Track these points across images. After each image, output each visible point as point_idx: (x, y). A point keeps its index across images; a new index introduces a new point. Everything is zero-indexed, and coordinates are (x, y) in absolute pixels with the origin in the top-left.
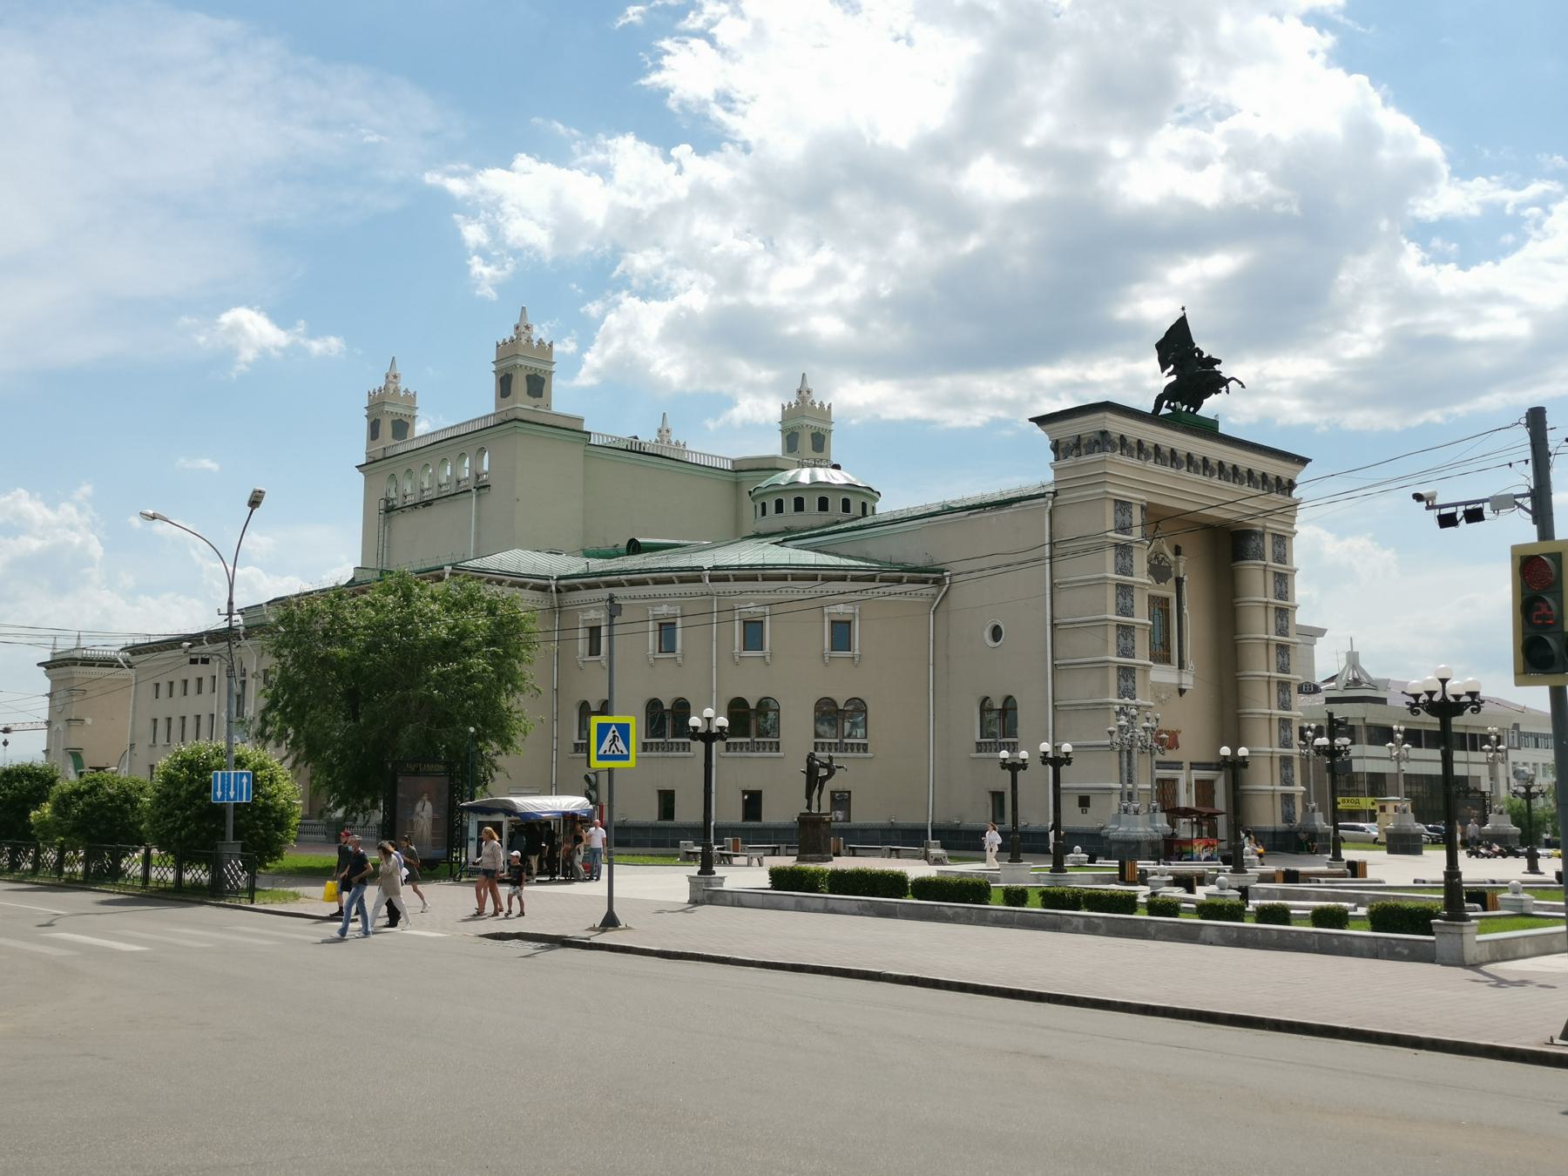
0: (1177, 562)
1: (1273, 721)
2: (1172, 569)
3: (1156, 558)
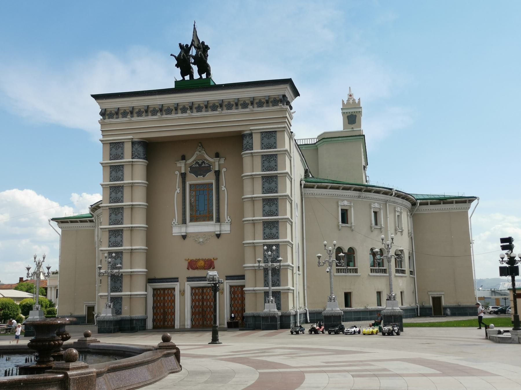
0: (215, 162)
1: (257, 249)
2: (211, 167)
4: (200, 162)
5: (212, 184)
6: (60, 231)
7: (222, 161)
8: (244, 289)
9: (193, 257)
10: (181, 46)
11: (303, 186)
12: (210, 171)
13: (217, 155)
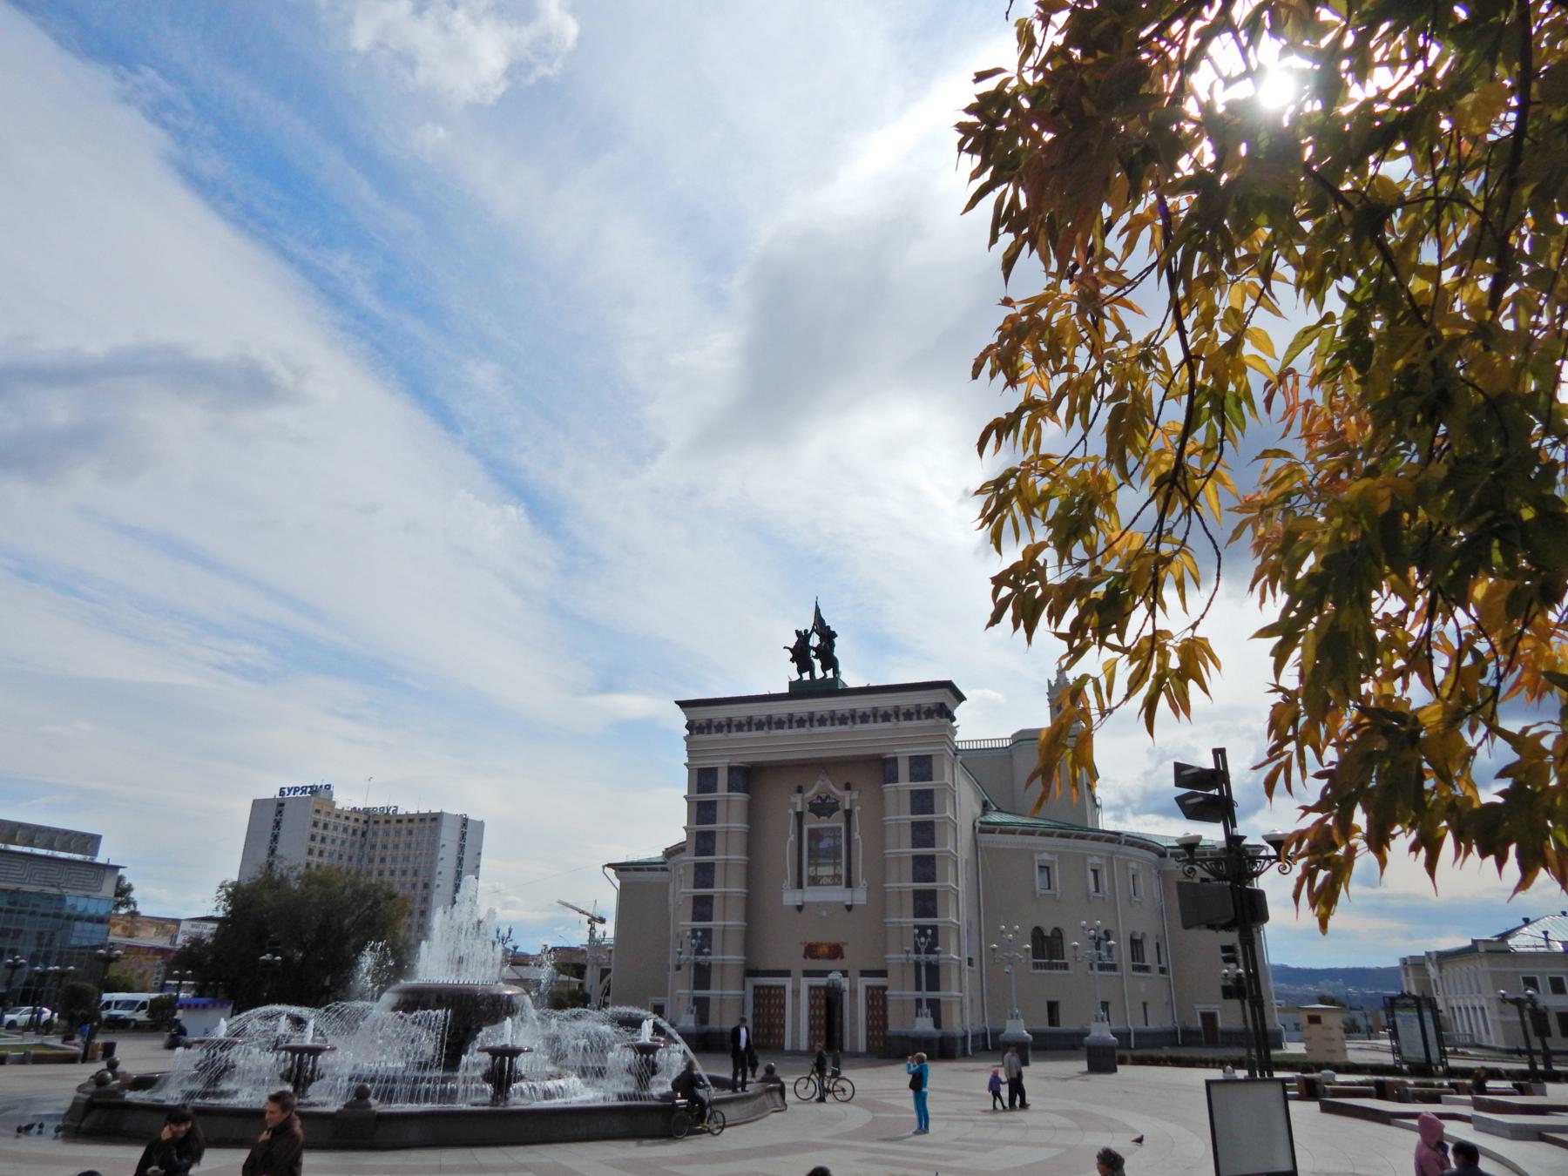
3: (819, 797)
4: (823, 796)
5: (840, 829)
6: (617, 883)
7: (855, 796)
8: (887, 993)
9: (812, 940)
10: (798, 633)
11: (977, 830)
12: (838, 809)
13: (848, 787)
